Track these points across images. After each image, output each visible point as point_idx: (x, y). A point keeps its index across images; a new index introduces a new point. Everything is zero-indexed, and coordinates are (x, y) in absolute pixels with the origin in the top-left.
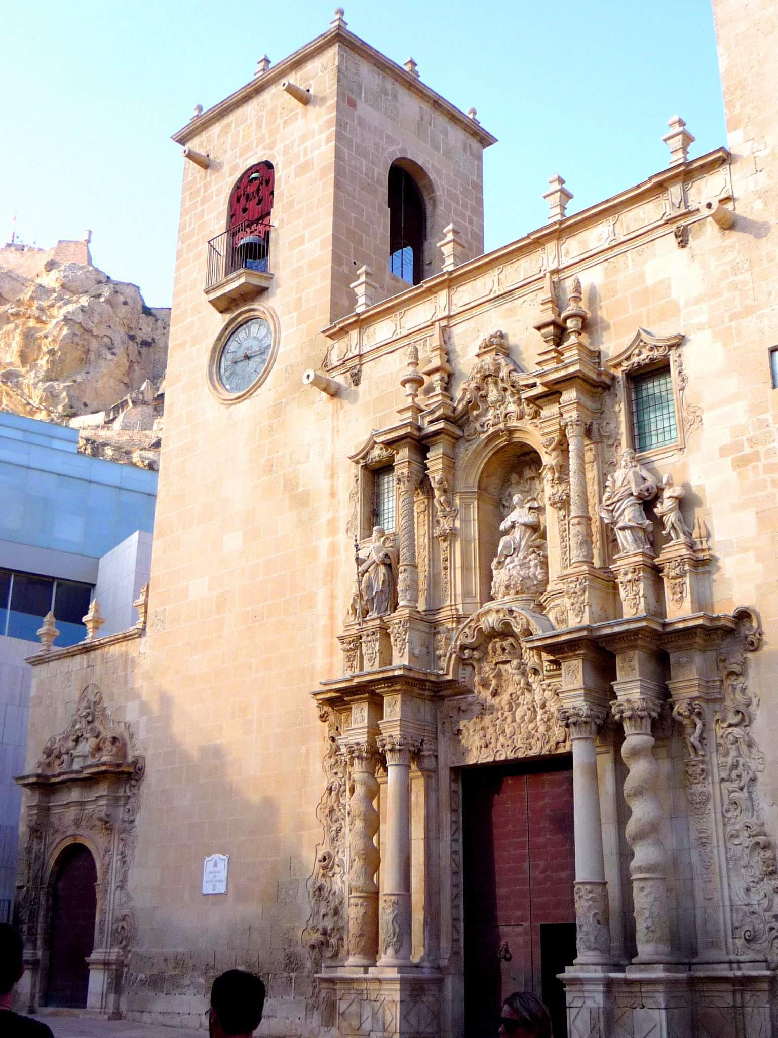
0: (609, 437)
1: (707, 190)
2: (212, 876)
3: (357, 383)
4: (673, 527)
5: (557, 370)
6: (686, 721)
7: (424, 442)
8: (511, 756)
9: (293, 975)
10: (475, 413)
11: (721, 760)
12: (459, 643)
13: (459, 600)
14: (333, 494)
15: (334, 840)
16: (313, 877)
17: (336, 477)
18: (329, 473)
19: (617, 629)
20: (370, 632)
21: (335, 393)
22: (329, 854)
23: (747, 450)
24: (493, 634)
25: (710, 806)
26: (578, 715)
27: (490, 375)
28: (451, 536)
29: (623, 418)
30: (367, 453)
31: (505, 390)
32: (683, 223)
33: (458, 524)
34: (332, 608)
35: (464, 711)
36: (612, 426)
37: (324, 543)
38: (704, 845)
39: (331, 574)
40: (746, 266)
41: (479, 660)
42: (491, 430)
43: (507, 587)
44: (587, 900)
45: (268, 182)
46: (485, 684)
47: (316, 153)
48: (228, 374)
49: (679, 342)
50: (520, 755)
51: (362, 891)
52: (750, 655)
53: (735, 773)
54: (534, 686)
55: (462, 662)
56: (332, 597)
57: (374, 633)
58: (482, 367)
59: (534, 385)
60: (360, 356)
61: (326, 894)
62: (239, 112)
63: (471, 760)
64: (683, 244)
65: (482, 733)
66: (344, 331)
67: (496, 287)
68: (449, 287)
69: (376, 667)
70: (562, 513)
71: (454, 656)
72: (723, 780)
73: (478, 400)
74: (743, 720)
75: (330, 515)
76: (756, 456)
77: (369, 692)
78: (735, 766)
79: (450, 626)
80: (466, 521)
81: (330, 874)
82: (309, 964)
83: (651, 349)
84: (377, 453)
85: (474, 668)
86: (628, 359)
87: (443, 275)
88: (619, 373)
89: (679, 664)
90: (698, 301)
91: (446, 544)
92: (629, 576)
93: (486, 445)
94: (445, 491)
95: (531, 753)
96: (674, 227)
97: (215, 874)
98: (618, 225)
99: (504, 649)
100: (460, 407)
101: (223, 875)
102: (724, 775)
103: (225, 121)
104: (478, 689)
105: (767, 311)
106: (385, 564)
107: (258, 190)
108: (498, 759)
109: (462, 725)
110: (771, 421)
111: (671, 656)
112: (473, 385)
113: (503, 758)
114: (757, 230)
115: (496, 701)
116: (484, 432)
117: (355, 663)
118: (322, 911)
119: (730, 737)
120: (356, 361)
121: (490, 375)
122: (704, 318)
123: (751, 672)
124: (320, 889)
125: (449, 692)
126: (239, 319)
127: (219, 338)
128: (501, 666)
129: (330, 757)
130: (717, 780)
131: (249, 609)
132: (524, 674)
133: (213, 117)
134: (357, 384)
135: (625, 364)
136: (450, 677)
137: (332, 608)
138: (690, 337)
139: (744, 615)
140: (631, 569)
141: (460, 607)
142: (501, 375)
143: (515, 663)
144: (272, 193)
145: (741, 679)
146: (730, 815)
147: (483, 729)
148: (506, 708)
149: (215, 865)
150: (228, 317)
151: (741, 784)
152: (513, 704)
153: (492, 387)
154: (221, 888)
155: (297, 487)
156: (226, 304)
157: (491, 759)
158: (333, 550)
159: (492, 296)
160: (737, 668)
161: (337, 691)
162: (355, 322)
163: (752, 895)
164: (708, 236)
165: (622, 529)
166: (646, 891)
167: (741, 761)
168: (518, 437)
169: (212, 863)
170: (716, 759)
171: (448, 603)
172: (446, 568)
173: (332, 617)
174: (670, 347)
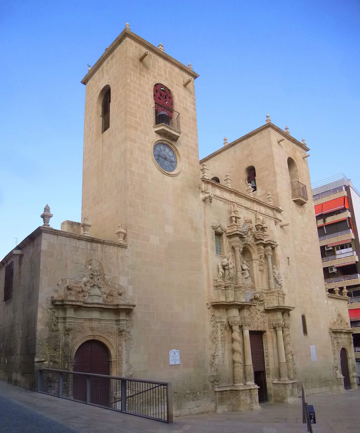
2: (174, 358)
9: (206, 391)
14: (206, 234)
39: (207, 261)
82: (211, 387)
97: (174, 357)
101: (178, 358)
118: (213, 370)
126: (164, 142)
149: (175, 354)
158: (207, 252)
169: (173, 353)
173: (208, 275)
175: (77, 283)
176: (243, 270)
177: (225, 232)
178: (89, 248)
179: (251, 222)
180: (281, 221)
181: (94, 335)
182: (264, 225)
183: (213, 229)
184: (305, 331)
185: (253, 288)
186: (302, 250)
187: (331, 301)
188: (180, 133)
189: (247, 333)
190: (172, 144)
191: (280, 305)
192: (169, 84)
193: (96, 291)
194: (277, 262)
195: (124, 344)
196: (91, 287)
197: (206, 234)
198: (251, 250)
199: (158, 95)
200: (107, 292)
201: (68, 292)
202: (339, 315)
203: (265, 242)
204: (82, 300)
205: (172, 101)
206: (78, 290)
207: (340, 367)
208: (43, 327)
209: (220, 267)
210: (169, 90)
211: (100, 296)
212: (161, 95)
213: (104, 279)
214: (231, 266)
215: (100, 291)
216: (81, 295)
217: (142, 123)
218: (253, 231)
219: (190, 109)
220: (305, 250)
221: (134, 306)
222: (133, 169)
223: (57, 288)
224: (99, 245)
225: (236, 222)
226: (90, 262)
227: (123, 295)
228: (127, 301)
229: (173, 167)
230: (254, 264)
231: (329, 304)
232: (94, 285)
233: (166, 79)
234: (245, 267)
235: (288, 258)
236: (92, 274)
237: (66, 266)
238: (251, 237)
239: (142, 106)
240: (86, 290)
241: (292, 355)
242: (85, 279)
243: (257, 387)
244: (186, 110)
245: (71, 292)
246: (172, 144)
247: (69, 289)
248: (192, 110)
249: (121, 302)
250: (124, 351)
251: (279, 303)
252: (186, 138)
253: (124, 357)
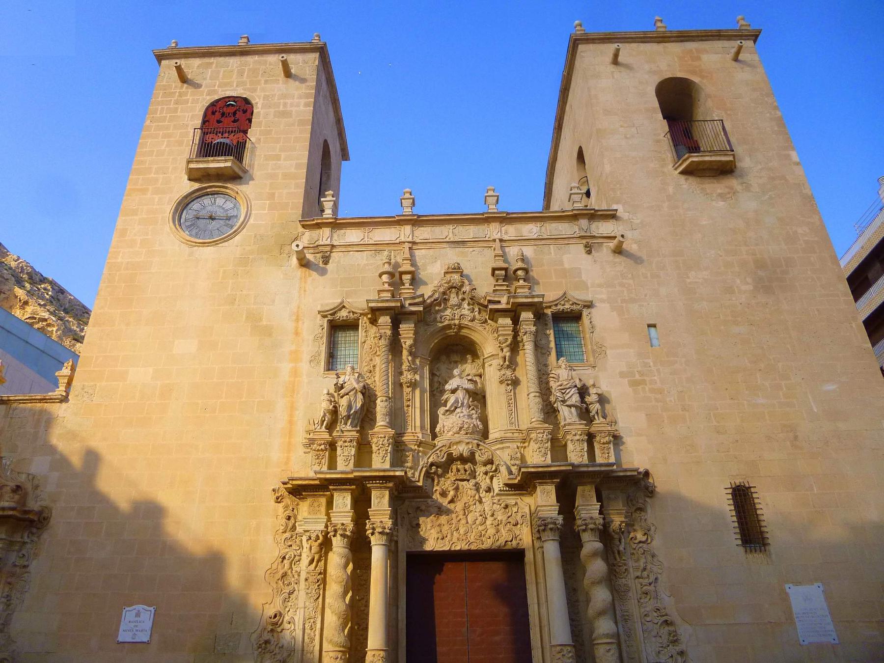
0: (542, 348)
1: (604, 228)
3: (326, 262)
4: (597, 413)
5: (526, 297)
6: (616, 536)
7: (399, 317)
8: (466, 548)
10: (437, 308)
11: (635, 564)
12: (431, 460)
13: (418, 430)
14: (297, 334)
15: (285, 601)
16: (259, 632)
17: (300, 322)
18: (294, 318)
19: (591, 469)
20: (348, 440)
21: (304, 263)
22: (281, 614)
23: (637, 377)
24: (463, 459)
25: (630, 594)
26: (555, 523)
27: (455, 287)
28: (413, 385)
29: (552, 338)
30: (335, 312)
31: (463, 299)
32: (591, 241)
33: (417, 377)
34: (291, 416)
35: (421, 510)
36: (543, 342)
37: (286, 367)
38: (626, 620)
40: (630, 276)
41: (439, 476)
42: (447, 323)
43: (461, 428)
44: (569, 658)
45: (245, 112)
46: (444, 494)
47: (294, 109)
48: (188, 224)
49: (589, 305)
50: (473, 547)
51: (343, 647)
52: (647, 499)
53: (645, 574)
54: (484, 500)
55: (428, 475)
56: (292, 408)
57: (351, 441)
58: (450, 281)
59: (499, 302)
60: (333, 246)
61: (273, 647)
62: (221, 59)
63: (429, 546)
64: (589, 252)
65: (438, 529)
66: (318, 226)
67: (451, 235)
68: (413, 225)
69: (348, 469)
70: (510, 387)
71: (424, 469)
72: (637, 577)
73: (444, 300)
74: (647, 539)
75: (293, 348)
76: (643, 382)
77: (322, 488)
78: (645, 569)
79: (413, 447)
80: (422, 377)
81: (279, 630)
83: (572, 304)
84: (343, 314)
85: (433, 480)
86: (556, 305)
87: (414, 215)
88: (548, 312)
89: (609, 499)
90: (600, 286)
91: (410, 389)
92: (578, 437)
93: (440, 331)
94: (411, 354)
95: (484, 547)
96: (584, 241)
98: (543, 228)
99: (466, 471)
100: (429, 301)
101: (148, 624)
102: (639, 574)
103: (207, 60)
104: (436, 496)
105: (645, 304)
106: (363, 394)
107: (234, 114)
108: (453, 549)
109: (422, 520)
110: (652, 364)
111: (603, 492)
112: (441, 290)
113: (458, 548)
114: (637, 260)
115: (451, 506)
116: (441, 322)
117: (323, 461)
119: (641, 550)
120: (328, 249)
121: (455, 287)
122: (604, 297)
123: (649, 511)
124: (267, 642)
125: (409, 495)
127: (186, 197)
128: (461, 483)
129: (285, 532)
130: (632, 576)
131: (200, 402)
132: (478, 490)
133: (197, 53)
134: (326, 264)
135: (554, 308)
136: (420, 484)
137: (291, 416)
138: (597, 304)
139: (647, 474)
140: (579, 433)
141: (420, 435)
142: (464, 289)
143: (472, 482)
144: (250, 121)
145: (643, 513)
146: (642, 601)
147: (439, 525)
148: (462, 513)
149: (138, 615)
150: (197, 186)
151: (651, 581)
152: (466, 509)
153: (453, 295)
154: (145, 639)
155: (261, 320)
156: (194, 176)
157: (447, 548)
158: (295, 373)
159: (447, 240)
160: (640, 505)
161: (320, 479)
162: (331, 223)
163: (661, 656)
164: (605, 251)
165: (570, 406)
166: (612, 652)
167: (648, 567)
168: (464, 332)
170: (631, 563)
171: (409, 430)
172: (408, 406)
173: (291, 422)
174: (585, 306)
183: (324, 317)
190: (226, 188)
198: (475, 337)
219: (294, 109)
238: (466, 306)
246: (226, 188)
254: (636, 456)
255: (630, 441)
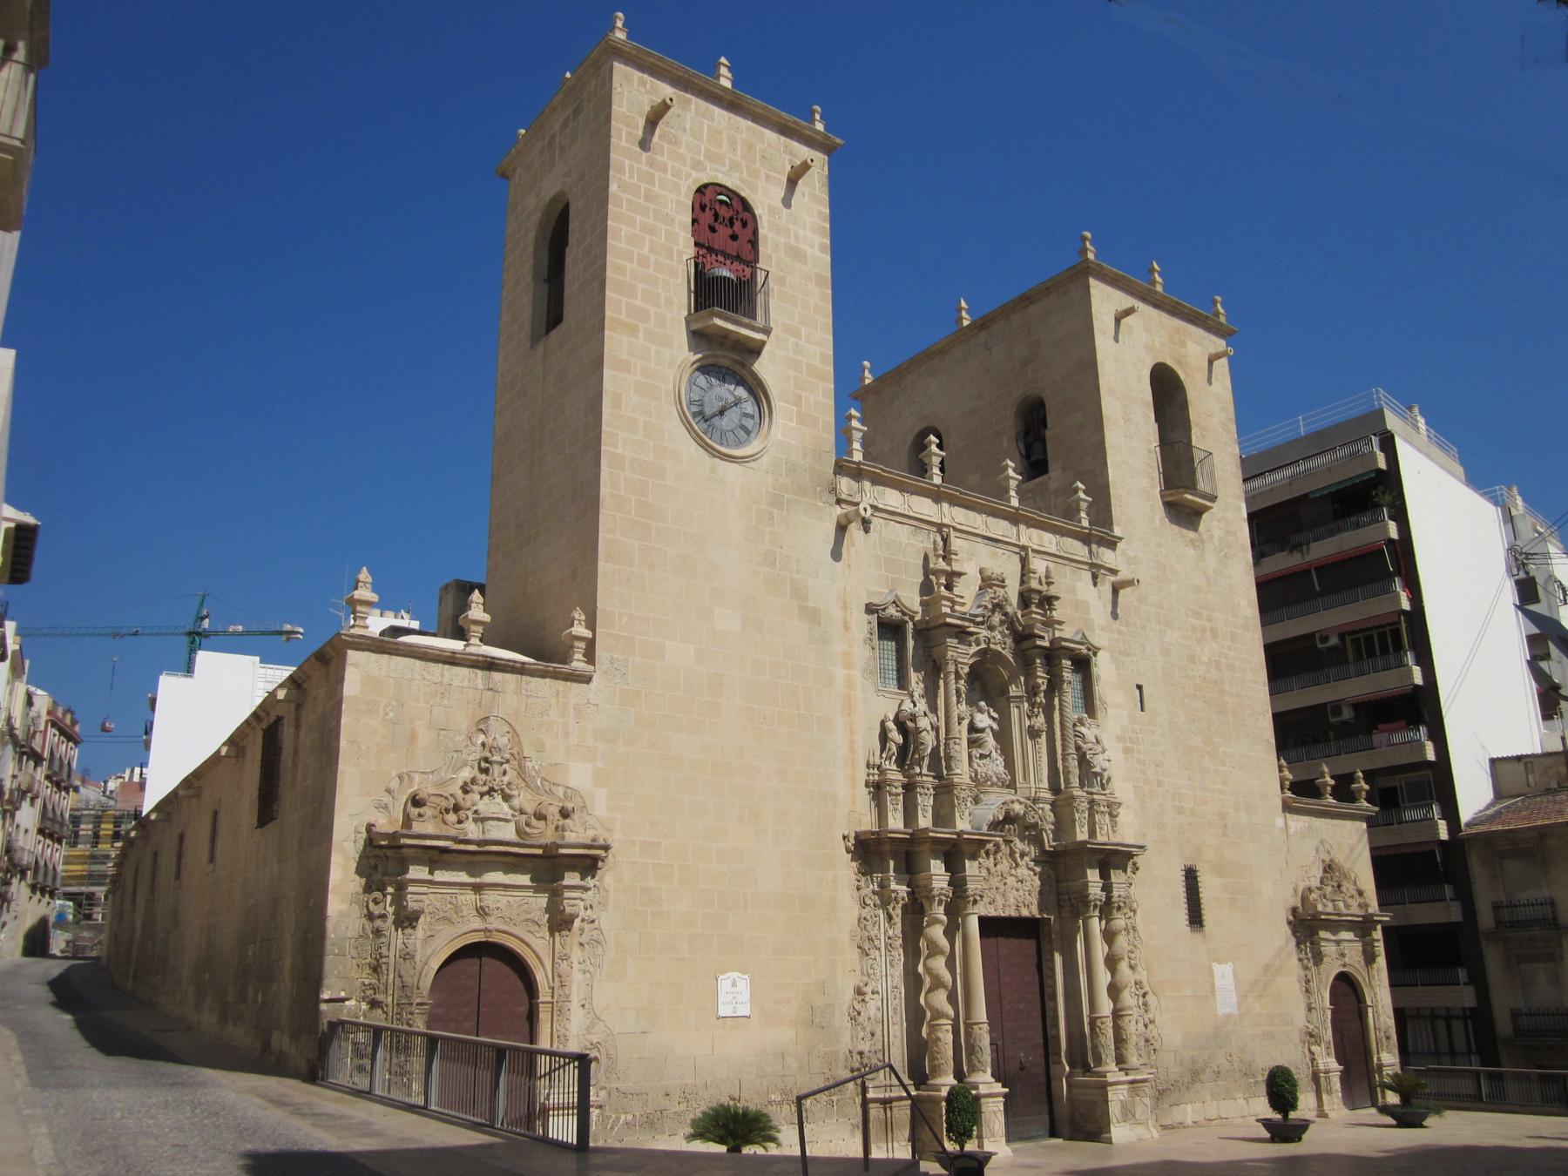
14: (846, 628)
34: (852, 742)
64: (1095, 584)
97: (735, 994)
101: (746, 996)
107: (732, 224)
137: (852, 742)
149: (734, 984)
154: (744, 1010)
158: (849, 683)
169: (729, 982)
173: (852, 750)
175: (443, 783)
176: (972, 728)
177: (912, 618)
178: (480, 686)
179: (1002, 583)
180: (1114, 572)
181: (486, 930)
182: (1053, 591)
184: (1196, 918)
185: (1012, 785)
186: (1192, 659)
187: (1298, 823)
188: (767, 331)
189: (973, 924)
191: (1100, 838)
192: (741, 179)
193: (496, 806)
194: (1097, 702)
195: (576, 954)
196: (482, 795)
197: (846, 628)
199: (707, 218)
200: (530, 808)
201: (414, 811)
202: (1329, 868)
203: (1047, 644)
204: (453, 832)
205: (755, 232)
206: (444, 804)
207: (1328, 1035)
208: (344, 907)
209: (891, 725)
210: (744, 201)
211: (507, 821)
212: (716, 216)
213: (521, 772)
214: (924, 723)
215: (511, 808)
216: (452, 817)
217: (653, 309)
218: (1009, 610)
219: (809, 250)
220: (1205, 659)
221: (606, 848)
222: (620, 451)
223: (387, 799)
224: (509, 676)
225: (949, 587)
226: (482, 725)
227: (575, 816)
228: (591, 833)
229: (748, 432)
230: (1015, 712)
231: (1291, 831)
232: (492, 790)
233: (735, 166)
234: (983, 720)
235: (1140, 687)
236: (486, 760)
237: (413, 737)
239: (653, 258)
240: (468, 804)
241: (1144, 995)
242: (466, 774)
243: (998, 1088)
244: (797, 254)
245: (422, 810)
247: (416, 802)
248: (818, 253)
249: (576, 835)
250: (577, 976)
251: (1092, 833)
252: (792, 340)
253: (576, 990)
254: (1125, 831)
255: (1124, 816)
